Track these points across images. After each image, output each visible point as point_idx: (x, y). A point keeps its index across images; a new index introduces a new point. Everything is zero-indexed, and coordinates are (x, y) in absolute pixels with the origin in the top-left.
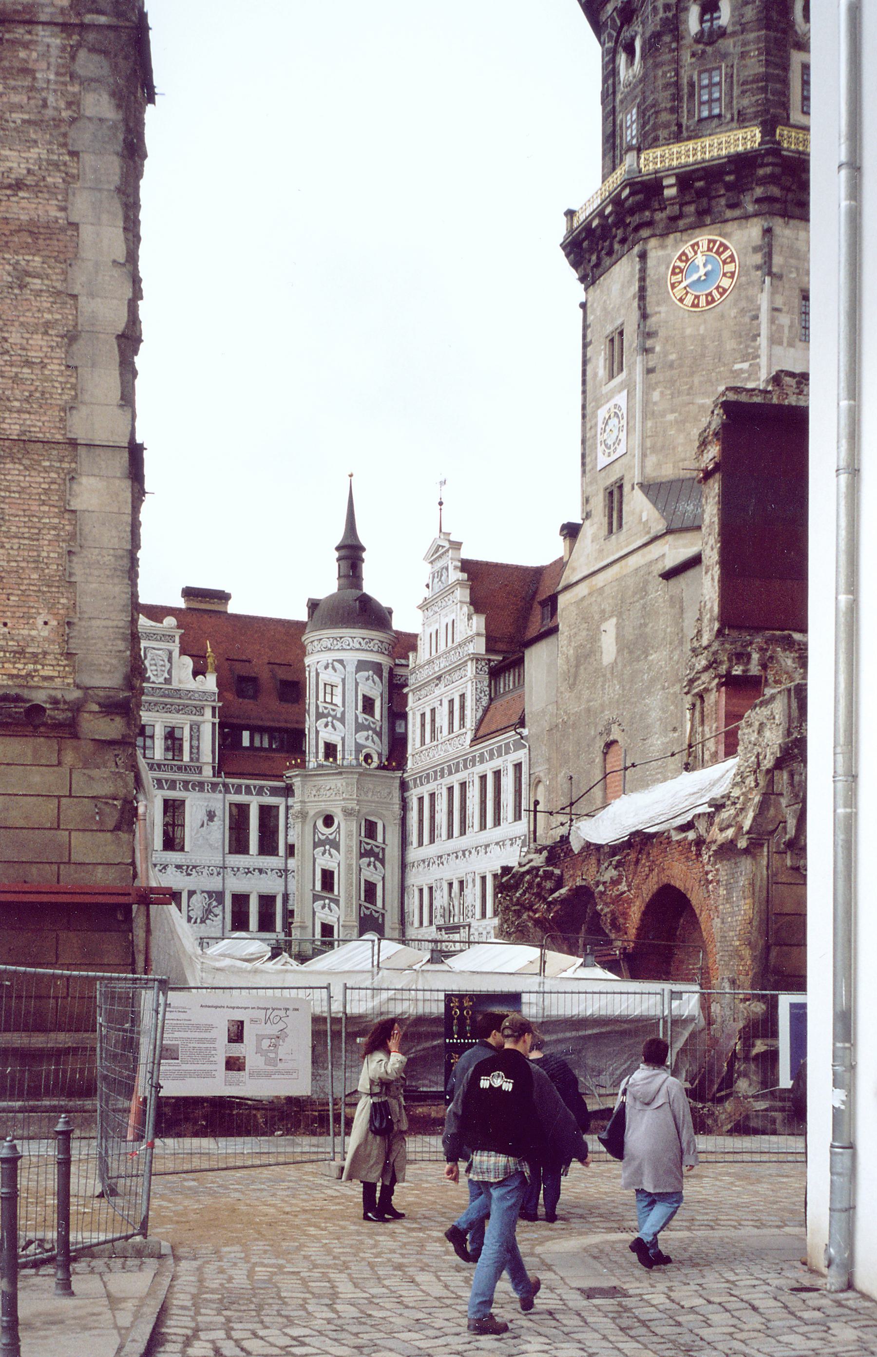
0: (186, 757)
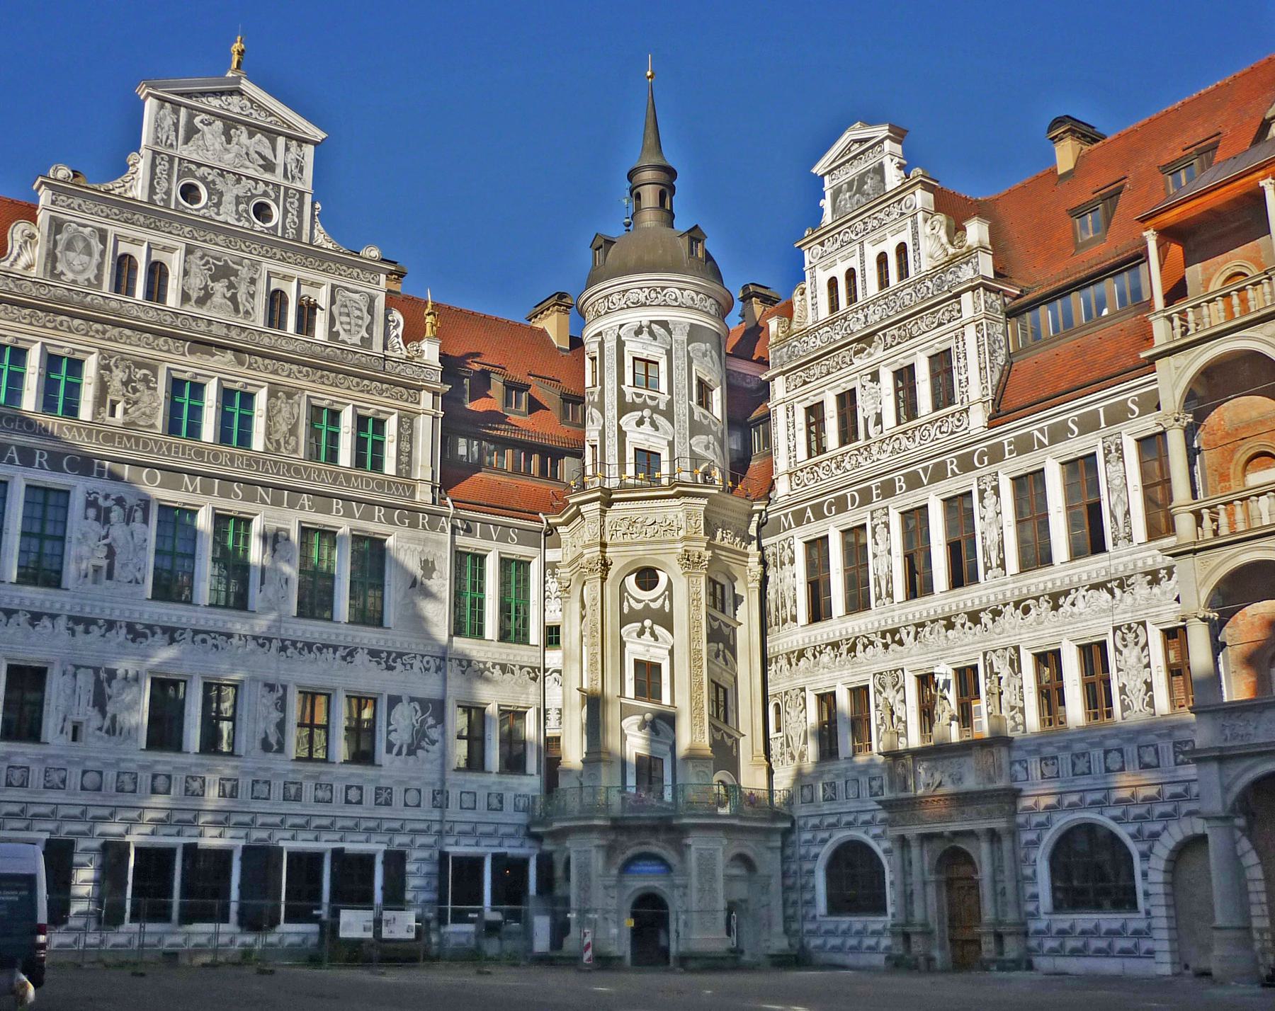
0: (390, 467)
